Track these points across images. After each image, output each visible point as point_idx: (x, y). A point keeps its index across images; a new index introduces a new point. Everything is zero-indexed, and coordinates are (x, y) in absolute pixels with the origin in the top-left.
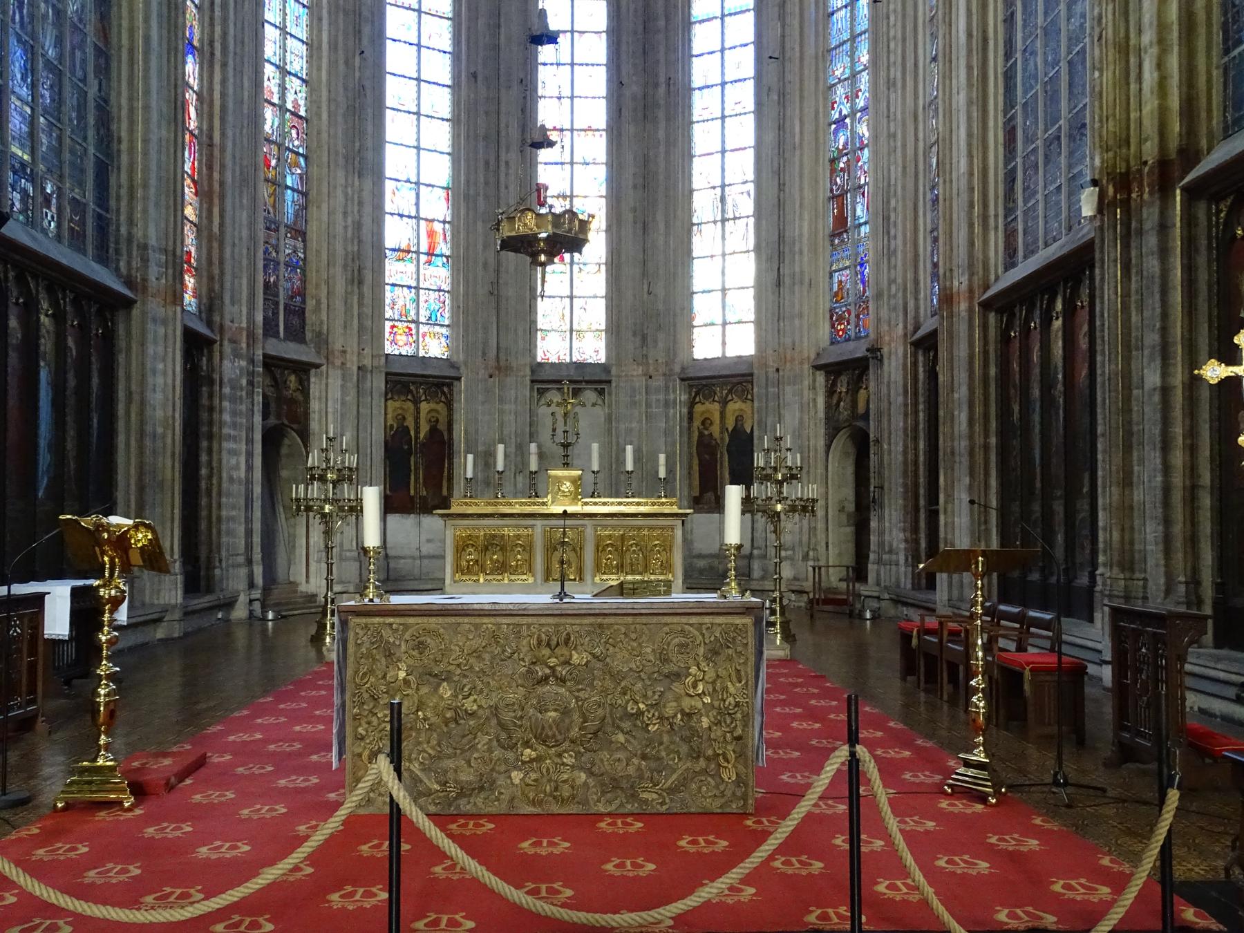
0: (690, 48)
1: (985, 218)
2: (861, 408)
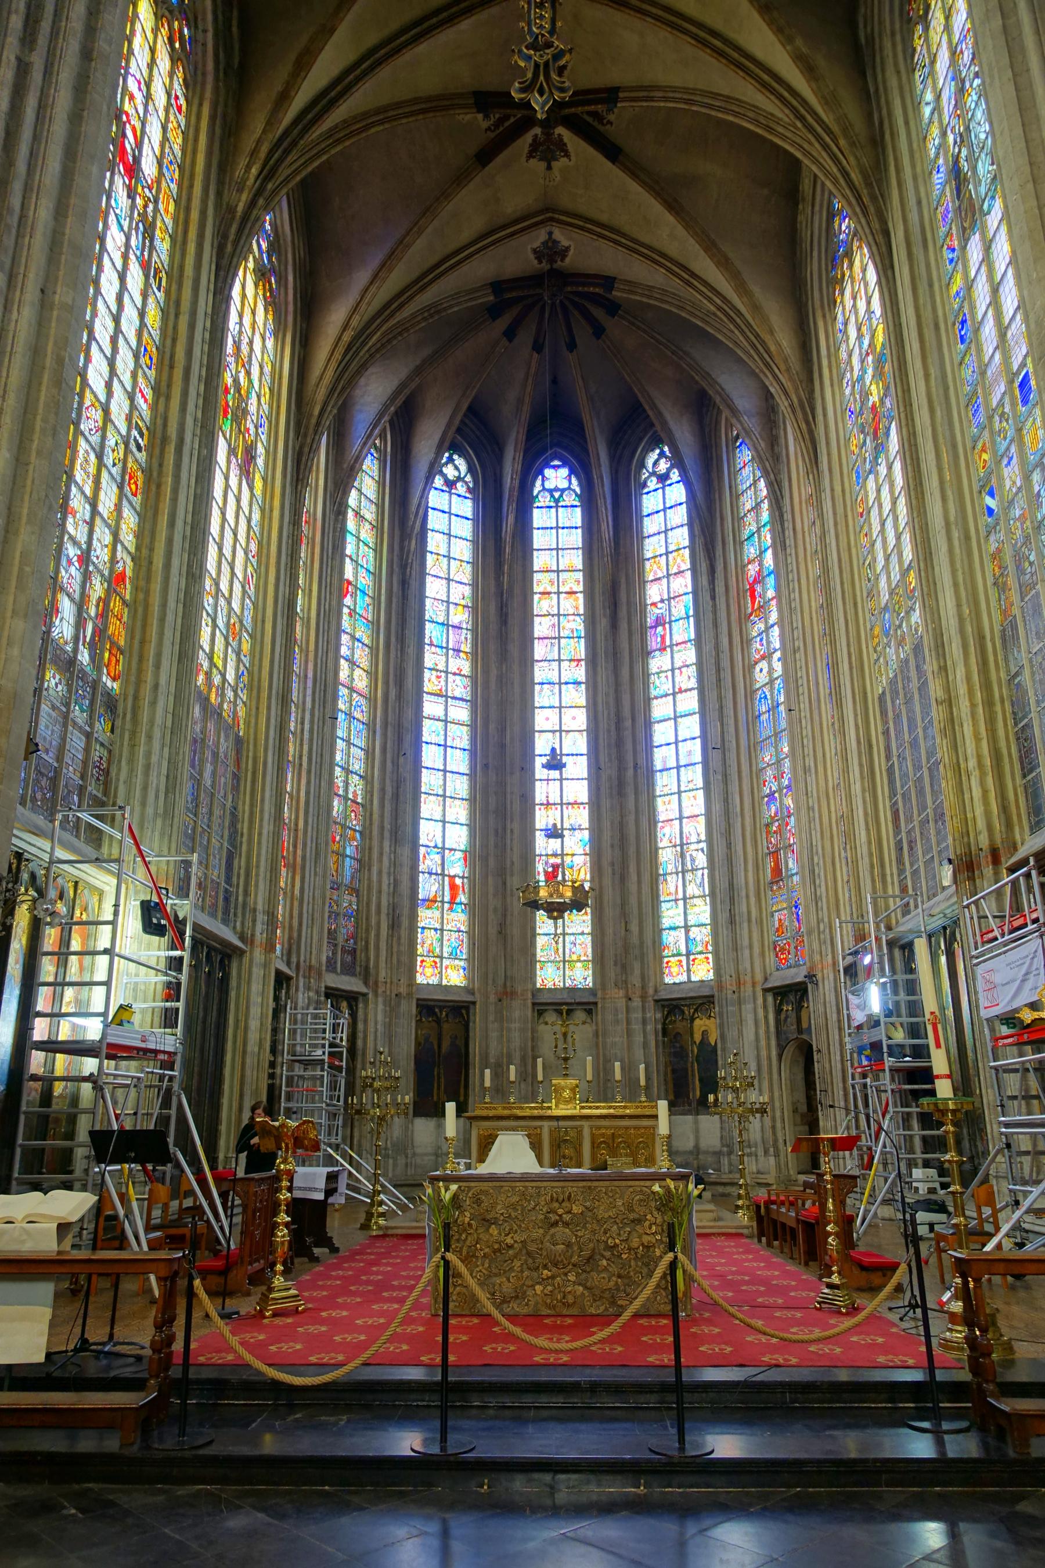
0: (651, 740)
1: (883, 876)
2: (805, 1025)
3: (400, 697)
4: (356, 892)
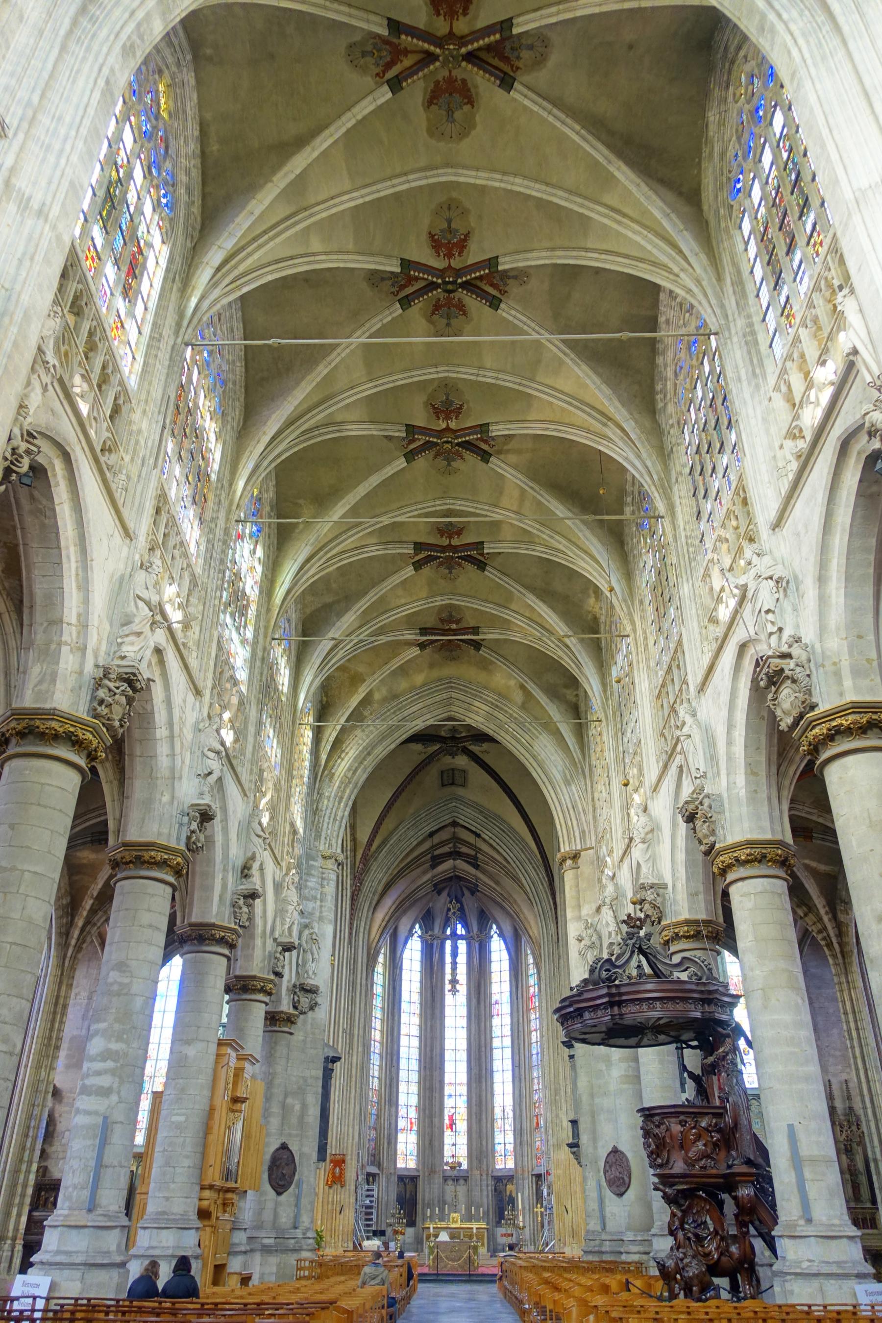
3: (392, 1040)
4: (375, 1129)
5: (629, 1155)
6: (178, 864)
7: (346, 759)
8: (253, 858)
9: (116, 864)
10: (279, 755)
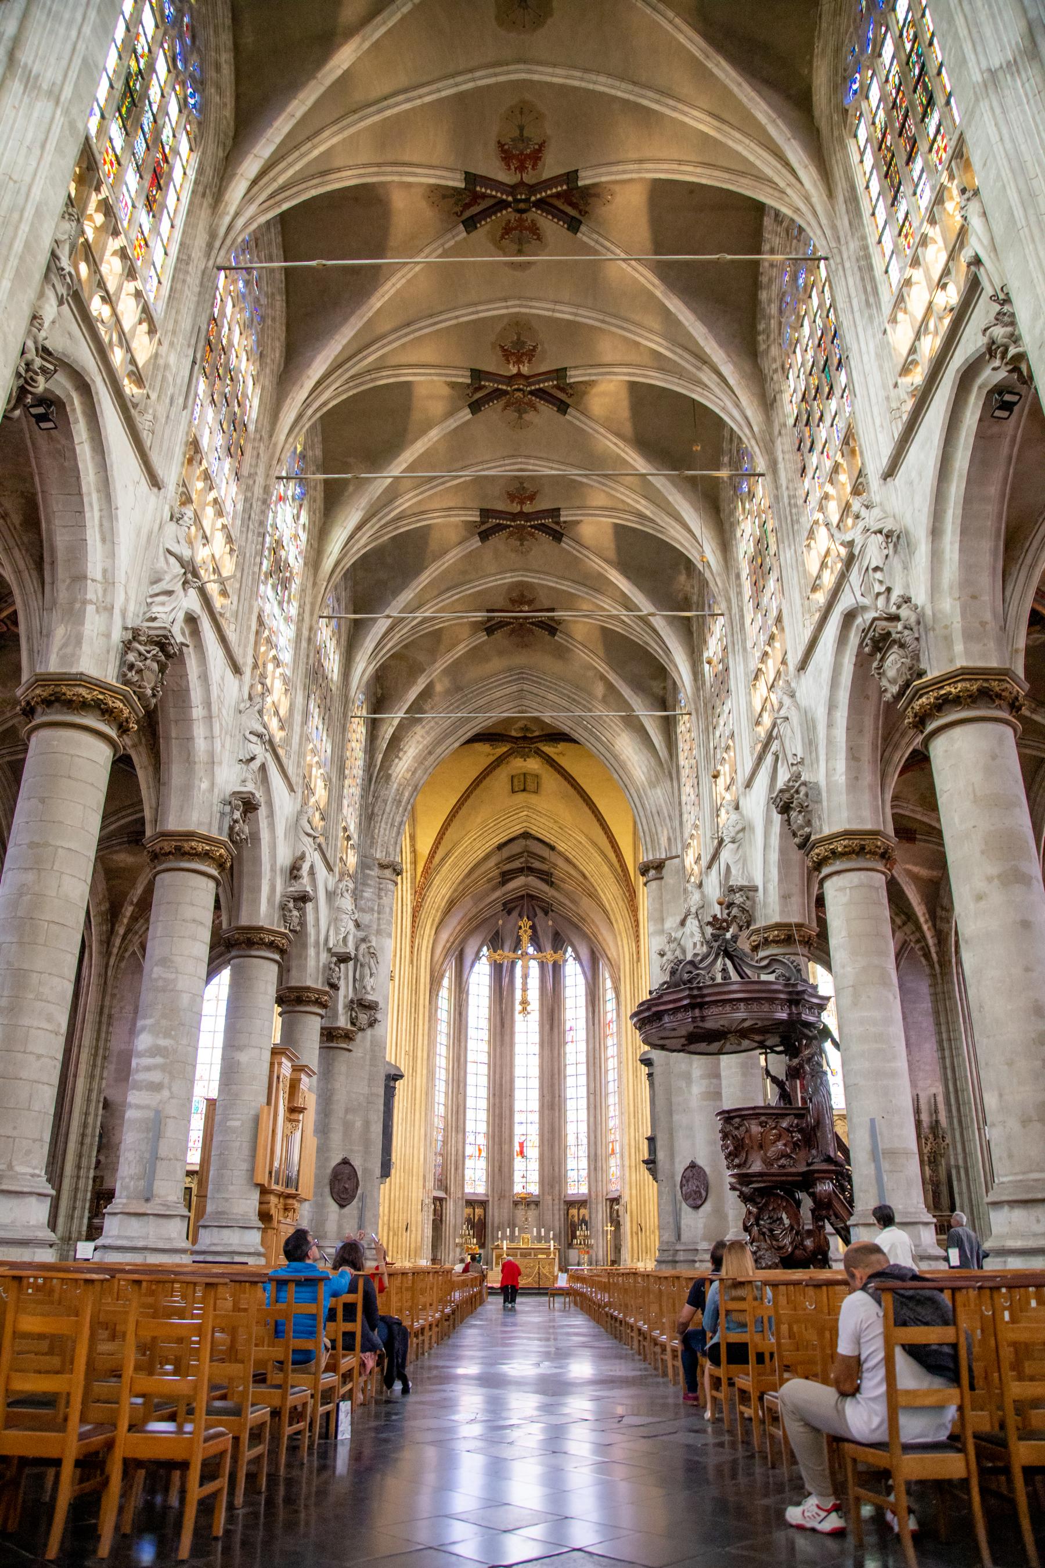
4: (441, 1155)
5: (707, 1170)
6: (221, 855)
7: (405, 758)
8: (302, 857)
9: (156, 857)
10: (329, 751)
